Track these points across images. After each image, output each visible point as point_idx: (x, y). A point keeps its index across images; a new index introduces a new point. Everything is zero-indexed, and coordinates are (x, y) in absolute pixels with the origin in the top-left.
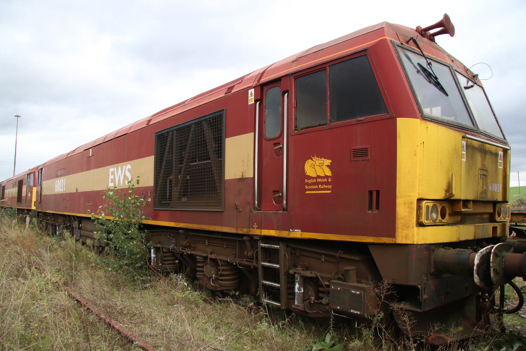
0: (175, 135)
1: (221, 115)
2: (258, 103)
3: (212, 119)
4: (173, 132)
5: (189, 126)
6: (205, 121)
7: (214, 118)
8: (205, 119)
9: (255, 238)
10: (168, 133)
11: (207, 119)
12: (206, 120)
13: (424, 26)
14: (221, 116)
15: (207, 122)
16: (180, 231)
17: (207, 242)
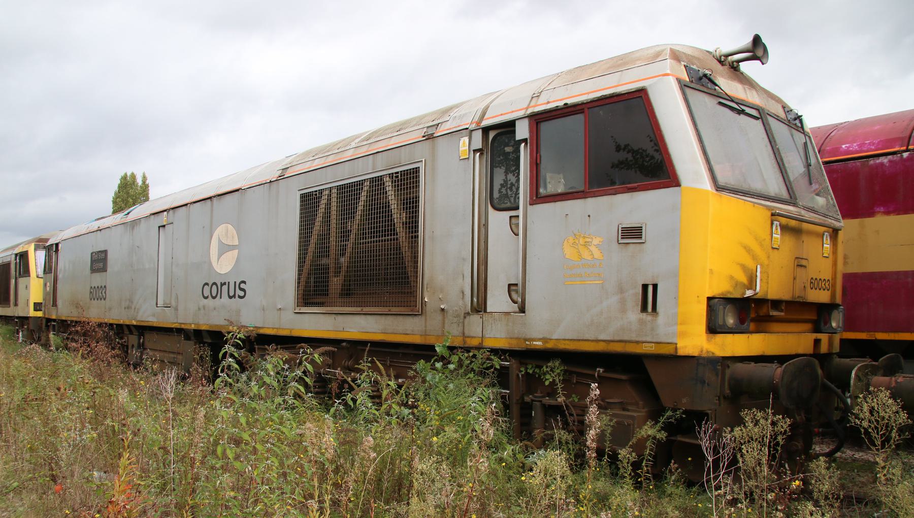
0: (334, 195)
1: (416, 168)
2: (478, 154)
3: (401, 175)
4: (331, 191)
5: (361, 183)
6: (390, 177)
7: (404, 173)
8: (390, 174)
10: (321, 191)
11: (393, 174)
12: (391, 175)
13: (725, 50)
14: (417, 170)
15: (392, 178)
16: (344, 344)
17: (389, 362)
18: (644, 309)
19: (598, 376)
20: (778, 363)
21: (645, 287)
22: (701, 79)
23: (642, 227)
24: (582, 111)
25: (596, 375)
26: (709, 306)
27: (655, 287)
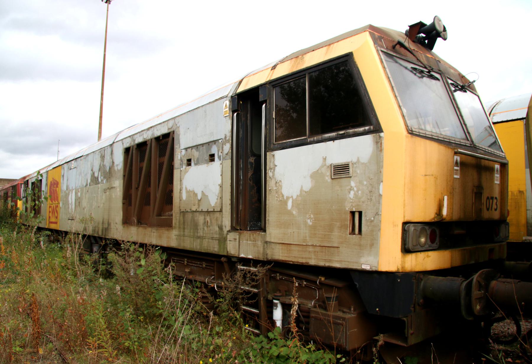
9: (233, 260)
17: (186, 262)
18: (353, 232)
19: (319, 283)
20: (462, 277)
21: (353, 213)
22: (394, 47)
23: (348, 164)
24: (304, 76)
25: (318, 283)
26: (405, 232)
27: (360, 213)
